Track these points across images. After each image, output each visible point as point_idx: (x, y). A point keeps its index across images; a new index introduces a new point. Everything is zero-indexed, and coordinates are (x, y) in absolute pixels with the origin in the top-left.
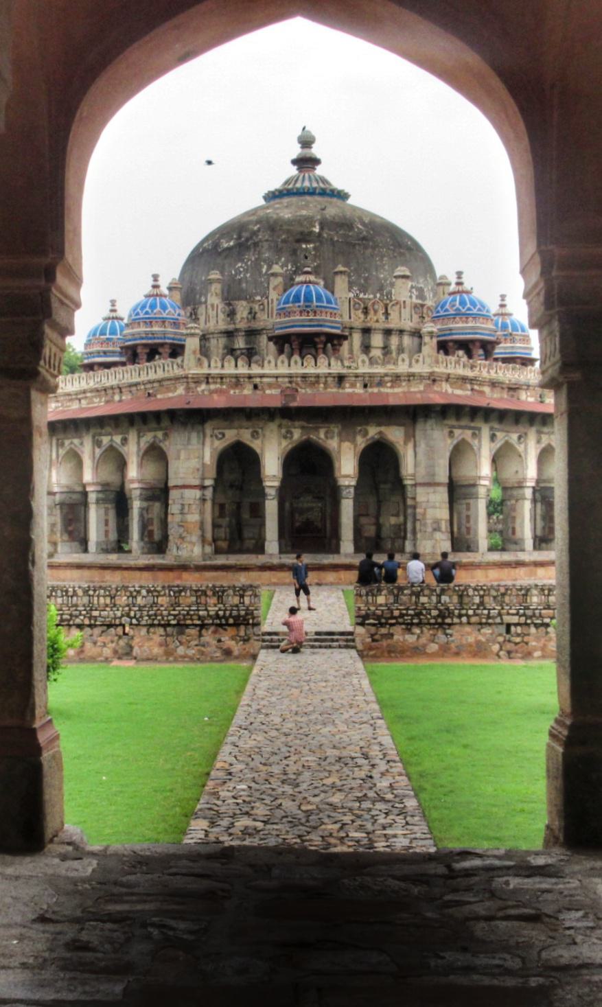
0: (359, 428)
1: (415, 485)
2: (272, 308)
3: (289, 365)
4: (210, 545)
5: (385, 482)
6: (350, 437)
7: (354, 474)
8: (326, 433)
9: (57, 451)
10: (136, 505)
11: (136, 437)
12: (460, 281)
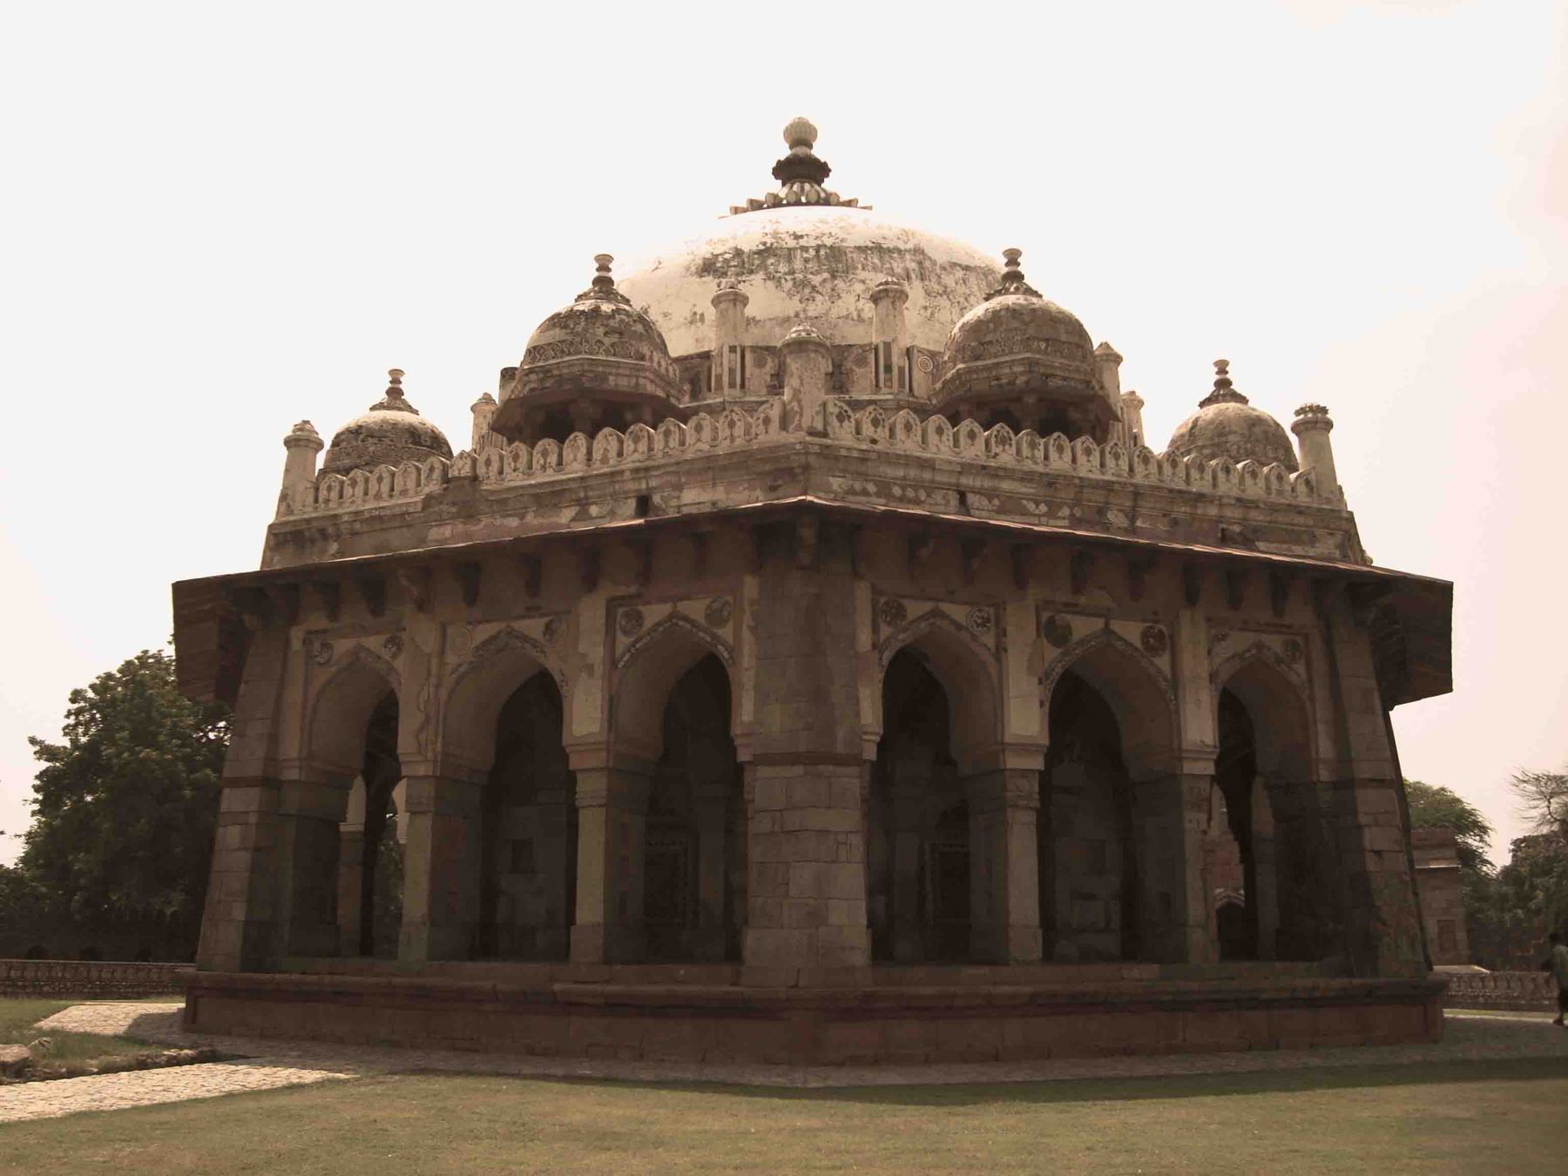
9: (875, 629)
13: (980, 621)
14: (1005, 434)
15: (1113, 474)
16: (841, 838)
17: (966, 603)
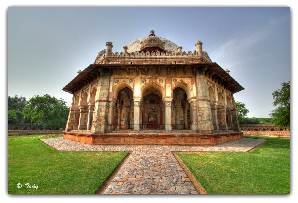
0: (173, 78)
1: (198, 100)
3: (145, 55)
4: (111, 126)
5: (178, 105)
7: (171, 96)
8: (160, 80)
10: (89, 111)
11: (90, 87)
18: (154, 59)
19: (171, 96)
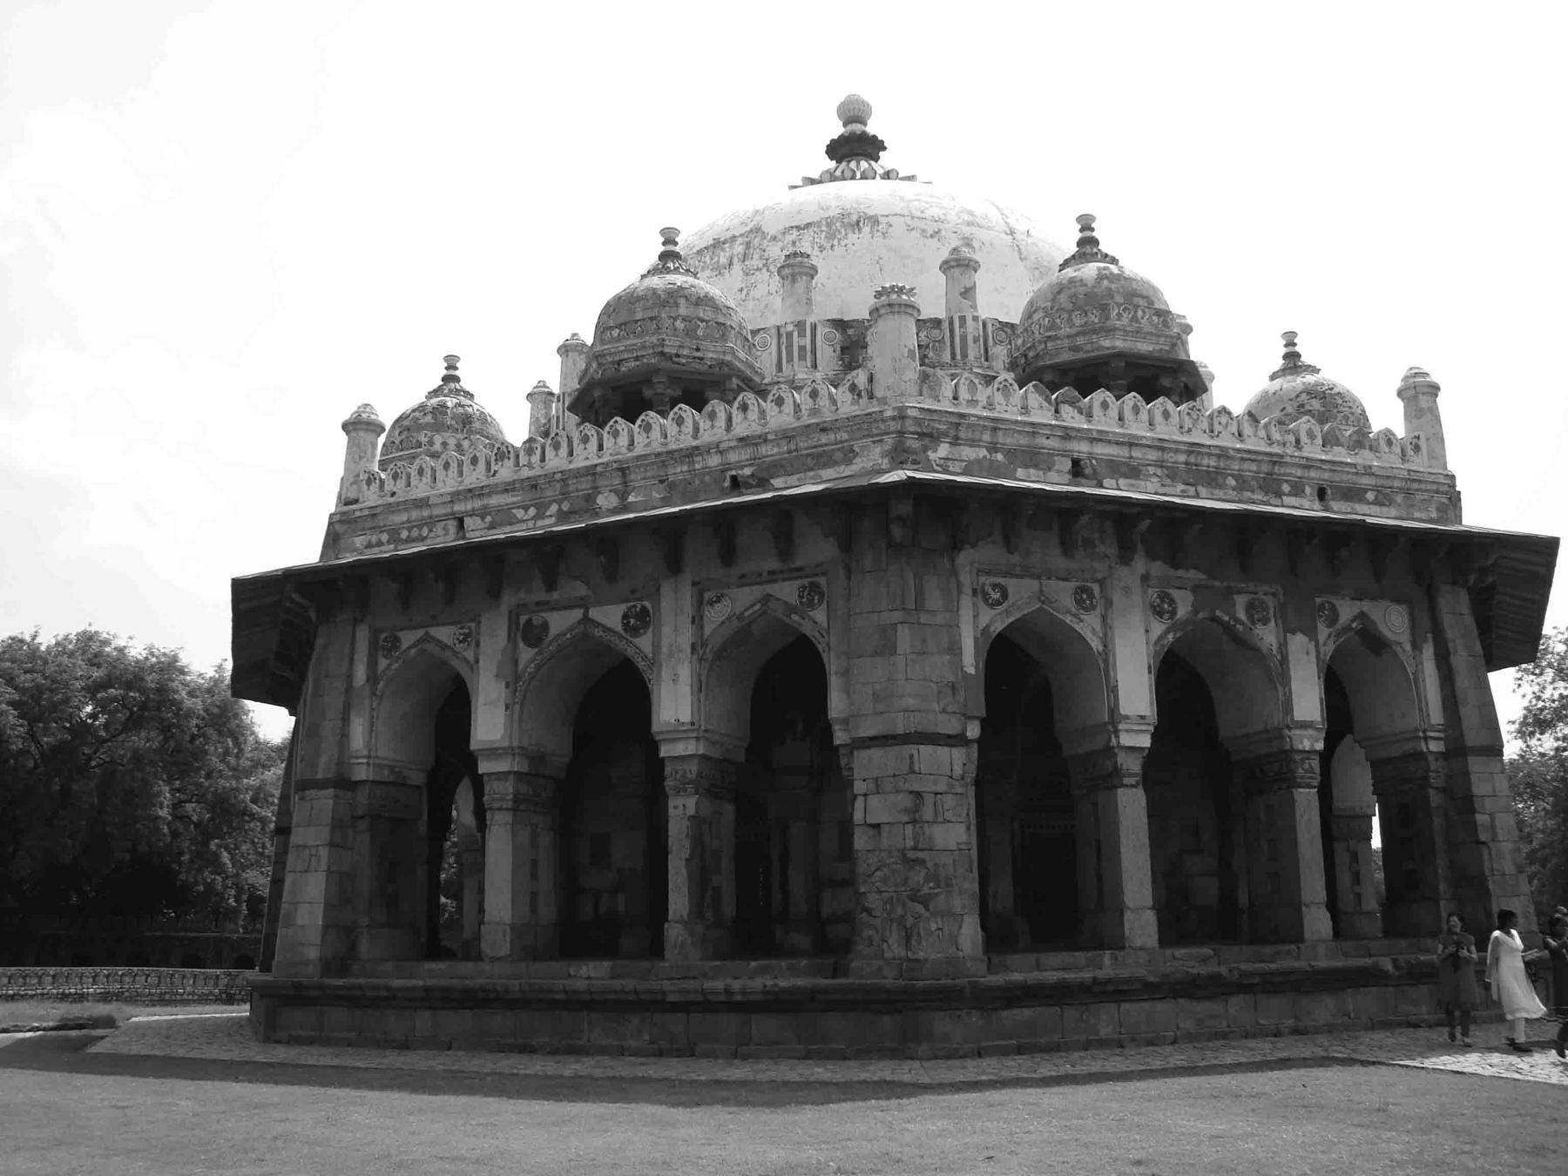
0: (1318, 600)
2: (964, 338)
6: (1298, 619)
8: (1250, 607)
9: (372, 664)
10: (682, 809)
12: (1290, 349)
13: (461, 638)
14: (505, 450)
15: (611, 454)
16: (314, 852)
17: (451, 624)
18: (1210, 455)
19: (1319, 719)
